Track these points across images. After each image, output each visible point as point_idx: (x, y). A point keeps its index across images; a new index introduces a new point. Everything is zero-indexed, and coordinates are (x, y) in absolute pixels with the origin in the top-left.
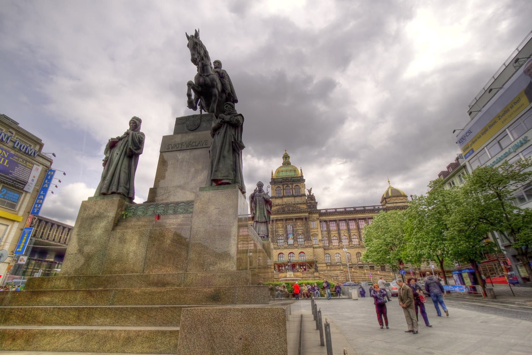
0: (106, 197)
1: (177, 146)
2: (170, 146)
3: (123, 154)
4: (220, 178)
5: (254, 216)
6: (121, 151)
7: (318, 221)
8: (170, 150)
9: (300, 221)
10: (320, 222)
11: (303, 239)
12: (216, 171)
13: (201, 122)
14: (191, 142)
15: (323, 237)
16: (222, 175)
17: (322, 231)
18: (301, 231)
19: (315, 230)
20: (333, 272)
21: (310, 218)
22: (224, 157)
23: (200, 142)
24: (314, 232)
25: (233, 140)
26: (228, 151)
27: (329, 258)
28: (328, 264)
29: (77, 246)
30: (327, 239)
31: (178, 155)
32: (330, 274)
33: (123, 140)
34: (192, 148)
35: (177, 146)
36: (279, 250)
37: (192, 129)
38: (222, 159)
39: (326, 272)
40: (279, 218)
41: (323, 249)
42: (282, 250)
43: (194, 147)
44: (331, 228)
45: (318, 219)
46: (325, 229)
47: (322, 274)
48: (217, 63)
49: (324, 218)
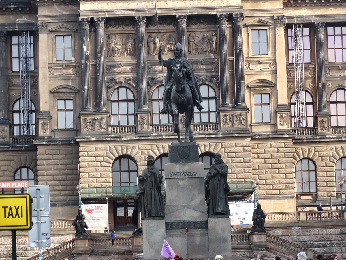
0: (155, 218)
1: (178, 174)
2: (172, 174)
3: (156, 189)
4: (220, 211)
5: (209, 202)
6: (153, 187)
7: (280, 32)
8: (173, 177)
9: (203, 27)
10: (288, 27)
11: (213, 102)
12: (218, 207)
13: (189, 152)
14: (187, 172)
15: (292, 93)
16: (221, 210)
17: (290, 68)
18: (207, 70)
19: (262, 67)
20: (316, 231)
21: (246, 14)
22: (221, 198)
23: (193, 172)
24: (260, 72)
25: (225, 188)
26: (223, 195)
27: (313, 174)
28: (303, 198)
29: (148, 245)
30: (309, 99)
31: (179, 182)
32: (305, 238)
33: (151, 177)
34: (189, 177)
35: (178, 174)
36: (118, 145)
37: (184, 158)
38: (220, 199)
39: (294, 230)
40: (120, 14)
41: (289, 142)
42: (130, 145)
43: (190, 177)
44: (331, 52)
45: (277, 20)
46: (307, 57)
47: (277, 237)
48: (179, 51)
49: (305, 12)
